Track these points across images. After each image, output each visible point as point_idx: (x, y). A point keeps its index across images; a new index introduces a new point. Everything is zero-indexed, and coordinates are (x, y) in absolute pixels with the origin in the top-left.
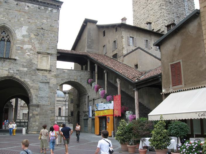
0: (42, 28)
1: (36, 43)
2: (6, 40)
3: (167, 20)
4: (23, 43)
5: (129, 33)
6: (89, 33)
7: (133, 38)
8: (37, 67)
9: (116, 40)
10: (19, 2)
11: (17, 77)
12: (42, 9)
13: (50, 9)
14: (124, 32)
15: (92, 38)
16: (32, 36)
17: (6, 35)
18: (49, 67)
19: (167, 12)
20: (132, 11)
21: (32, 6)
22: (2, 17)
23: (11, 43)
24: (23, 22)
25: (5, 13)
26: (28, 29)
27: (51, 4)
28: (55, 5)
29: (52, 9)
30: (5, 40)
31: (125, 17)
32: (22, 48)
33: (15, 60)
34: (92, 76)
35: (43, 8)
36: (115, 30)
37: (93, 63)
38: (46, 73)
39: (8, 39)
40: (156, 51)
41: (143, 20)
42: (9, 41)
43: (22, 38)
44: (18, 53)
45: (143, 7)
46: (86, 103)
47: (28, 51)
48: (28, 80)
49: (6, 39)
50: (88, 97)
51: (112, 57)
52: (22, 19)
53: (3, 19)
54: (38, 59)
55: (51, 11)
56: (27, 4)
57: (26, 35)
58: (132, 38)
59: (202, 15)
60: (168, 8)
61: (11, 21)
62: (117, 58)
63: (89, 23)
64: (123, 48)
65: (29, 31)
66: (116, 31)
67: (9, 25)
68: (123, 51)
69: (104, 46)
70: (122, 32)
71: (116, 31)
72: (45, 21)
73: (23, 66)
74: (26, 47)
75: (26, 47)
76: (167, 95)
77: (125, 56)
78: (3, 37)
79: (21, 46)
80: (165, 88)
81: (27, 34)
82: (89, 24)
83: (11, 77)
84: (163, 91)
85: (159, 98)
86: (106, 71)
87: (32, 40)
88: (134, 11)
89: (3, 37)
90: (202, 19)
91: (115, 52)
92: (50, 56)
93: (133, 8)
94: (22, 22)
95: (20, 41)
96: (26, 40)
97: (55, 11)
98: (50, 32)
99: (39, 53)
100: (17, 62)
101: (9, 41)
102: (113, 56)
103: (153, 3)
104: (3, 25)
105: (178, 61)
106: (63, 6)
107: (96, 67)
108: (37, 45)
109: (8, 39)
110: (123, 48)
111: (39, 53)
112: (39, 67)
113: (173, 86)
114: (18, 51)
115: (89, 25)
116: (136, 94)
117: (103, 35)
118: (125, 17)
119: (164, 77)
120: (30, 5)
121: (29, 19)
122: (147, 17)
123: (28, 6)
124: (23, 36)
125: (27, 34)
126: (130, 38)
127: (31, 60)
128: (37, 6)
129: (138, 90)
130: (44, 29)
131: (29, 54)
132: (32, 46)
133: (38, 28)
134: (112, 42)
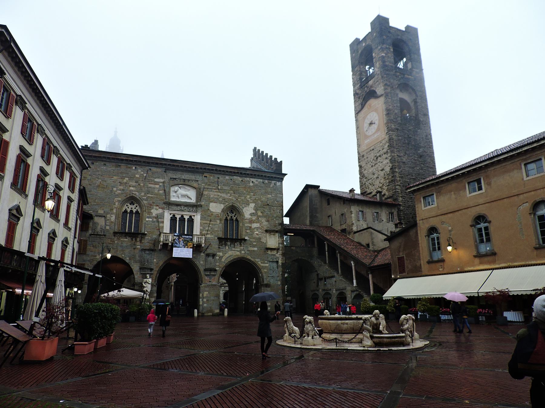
0: (268, 204)
1: (263, 220)
2: (234, 220)
3: (399, 186)
4: (251, 222)
5: (358, 207)
6: (311, 201)
7: (362, 212)
8: (266, 246)
9: (344, 213)
10: (243, 178)
11: (249, 257)
12: (266, 183)
13: (273, 182)
14: (353, 206)
15: (314, 206)
16: (259, 213)
17: (234, 215)
19: (400, 175)
20: (358, 166)
21: (257, 181)
23: (239, 223)
24: (249, 199)
25: (232, 192)
26: (255, 206)
27: (275, 178)
28: (278, 178)
29: (275, 182)
30: (233, 219)
31: (353, 189)
32: (250, 227)
33: (245, 240)
34: (321, 253)
35: (266, 181)
36: (342, 203)
37: (322, 240)
38: (274, 252)
40: (388, 224)
41: (372, 180)
42: (237, 220)
43: (250, 217)
44: (248, 233)
45: (372, 164)
46: (314, 281)
48: (259, 260)
49: (234, 218)
50: (318, 275)
51: (340, 231)
52: (249, 196)
53: (230, 198)
54: (266, 238)
55: (275, 184)
56: (252, 180)
57: (253, 213)
58: (361, 212)
59: (418, 225)
60: (400, 170)
61: (238, 200)
62: (346, 233)
63: (311, 189)
64: (353, 224)
65: (256, 209)
66: (344, 204)
67: (237, 205)
68: (353, 227)
69: (329, 216)
70: (350, 207)
71: (344, 204)
72: (270, 196)
73: (254, 246)
75: (255, 225)
76: (395, 280)
77: (355, 233)
78: (231, 217)
79: (250, 225)
80: (393, 275)
81: (254, 211)
82: (310, 190)
83: (243, 258)
84: (393, 276)
85: (390, 283)
86: (339, 251)
87: (260, 218)
88: (360, 167)
89: (231, 217)
90: (419, 228)
91: (344, 227)
92: (277, 234)
93: (359, 162)
94: (248, 199)
95: (248, 219)
97: (278, 184)
98: (275, 208)
99: (267, 231)
100: (247, 242)
102: (341, 230)
103: (384, 163)
104: (231, 204)
105: (402, 256)
106: (285, 178)
107: (326, 245)
108: (265, 223)
109: (236, 218)
110: (353, 224)
111: (267, 231)
112: (268, 246)
113: (400, 273)
114: (248, 231)
115: (311, 192)
116: (370, 276)
117: (327, 204)
118: (353, 189)
119: (393, 267)
120: (254, 180)
121: (255, 195)
122: (377, 178)
123: (252, 182)
124: (251, 214)
125: (254, 211)
126: (359, 212)
127: (260, 239)
128: (261, 180)
129: (371, 273)
130: (270, 206)
131: (258, 233)
132: (260, 225)
133: (264, 204)
134: (338, 215)
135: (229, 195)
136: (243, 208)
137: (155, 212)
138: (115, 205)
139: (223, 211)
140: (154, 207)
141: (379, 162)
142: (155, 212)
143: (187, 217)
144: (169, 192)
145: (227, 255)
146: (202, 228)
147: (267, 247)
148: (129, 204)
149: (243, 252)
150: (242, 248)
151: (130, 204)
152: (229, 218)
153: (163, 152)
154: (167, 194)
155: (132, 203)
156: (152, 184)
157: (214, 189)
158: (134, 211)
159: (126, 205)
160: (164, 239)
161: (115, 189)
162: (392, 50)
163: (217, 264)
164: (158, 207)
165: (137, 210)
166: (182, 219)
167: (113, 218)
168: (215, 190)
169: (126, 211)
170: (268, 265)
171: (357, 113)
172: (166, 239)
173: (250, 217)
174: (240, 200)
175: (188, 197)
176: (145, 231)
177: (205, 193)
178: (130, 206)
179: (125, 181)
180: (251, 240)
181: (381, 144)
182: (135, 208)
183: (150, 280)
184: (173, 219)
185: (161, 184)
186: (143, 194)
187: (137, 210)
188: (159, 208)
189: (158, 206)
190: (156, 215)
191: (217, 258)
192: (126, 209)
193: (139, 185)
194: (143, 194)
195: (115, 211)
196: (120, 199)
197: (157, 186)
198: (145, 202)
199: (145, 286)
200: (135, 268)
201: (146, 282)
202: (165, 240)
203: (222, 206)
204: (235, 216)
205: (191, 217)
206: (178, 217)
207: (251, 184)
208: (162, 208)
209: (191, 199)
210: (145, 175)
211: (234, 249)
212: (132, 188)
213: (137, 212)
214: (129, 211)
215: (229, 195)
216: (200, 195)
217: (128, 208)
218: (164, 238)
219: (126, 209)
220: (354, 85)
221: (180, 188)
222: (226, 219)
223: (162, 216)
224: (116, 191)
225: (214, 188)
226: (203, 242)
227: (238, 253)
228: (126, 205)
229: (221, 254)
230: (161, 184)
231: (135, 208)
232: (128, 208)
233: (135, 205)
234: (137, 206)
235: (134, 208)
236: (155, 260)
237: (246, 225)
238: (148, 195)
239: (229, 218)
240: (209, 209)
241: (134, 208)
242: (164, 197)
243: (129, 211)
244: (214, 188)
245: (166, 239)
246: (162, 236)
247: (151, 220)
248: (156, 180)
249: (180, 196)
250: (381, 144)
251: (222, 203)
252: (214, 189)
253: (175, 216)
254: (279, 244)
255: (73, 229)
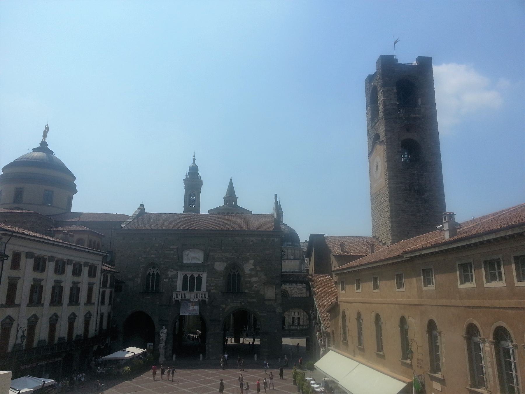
4: (251, 276)
16: (258, 268)
18: (274, 296)
22: (231, 255)
32: (250, 281)
33: (245, 293)
39: (238, 273)
42: (239, 275)
43: (249, 272)
47: (256, 283)
52: (248, 254)
53: (232, 256)
57: (253, 269)
61: (239, 258)
65: (255, 265)
72: (268, 252)
74: (254, 279)
75: (254, 279)
78: (234, 272)
81: (253, 267)
89: (234, 272)
96: (253, 273)
101: (239, 275)
109: (238, 273)
124: (251, 270)
125: (253, 267)
128: (260, 238)
131: (256, 286)
135: (231, 254)
136: (244, 264)
137: (170, 274)
138: (140, 270)
139: (226, 268)
140: (170, 270)
141: (382, 209)
142: (170, 274)
143: (196, 276)
144: (182, 257)
145: (229, 307)
146: (208, 284)
147: (265, 298)
148: (151, 269)
149: (243, 304)
150: (242, 300)
151: (153, 268)
152: (232, 274)
153: (231, 177)
154: (180, 257)
155: (154, 268)
156: (168, 251)
157: (219, 250)
158: (156, 273)
159: (149, 269)
160: (176, 297)
161: (140, 258)
162: (395, 91)
163: (221, 315)
164: (173, 269)
165: (158, 272)
166: (192, 277)
167: (139, 281)
168: (219, 251)
169: (149, 274)
170: (266, 314)
171: (370, 154)
172: (177, 297)
173: (249, 272)
174: (241, 257)
175: (197, 259)
176: (162, 290)
177: (211, 254)
178: (152, 270)
179: (148, 250)
180: (251, 292)
181: (383, 191)
182: (156, 271)
183: (166, 331)
184: (185, 278)
185: (175, 250)
186: (161, 259)
187: (158, 272)
188: (174, 270)
189: (172, 268)
190: (172, 276)
191: (221, 309)
192: (149, 273)
193: (158, 252)
194: (161, 259)
195: (140, 275)
196: (144, 265)
197: (172, 252)
198: (163, 266)
199: (162, 335)
200: (156, 320)
201: (162, 333)
202: (176, 298)
203: (225, 264)
204: (237, 272)
205: (199, 275)
206: (189, 276)
207: (251, 243)
208: (177, 270)
209: (200, 260)
210: (163, 243)
211: (235, 301)
212: (153, 256)
213: (158, 274)
214: (151, 273)
215: (231, 254)
216: (207, 257)
217: (151, 271)
218: (176, 296)
219: (149, 273)
220: (368, 124)
221: (190, 251)
222: (230, 275)
223: (176, 276)
224: (141, 260)
225: (218, 249)
226: (207, 297)
227: (239, 305)
228: (149, 269)
229: (224, 306)
230: (175, 250)
231: (156, 271)
232: (151, 271)
233: (156, 268)
234: (157, 270)
235: (155, 271)
236: (171, 313)
237: (246, 279)
238: (165, 260)
239: (232, 274)
240: (213, 268)
241: (155, 271)
242: (178, 260)
243: (151, 274)
244: (218, 249)
245: (177, 297)
246: (174, 294)
247: (167, 280)
248: (172, 247)
249: (190, 258)
250: (383, 191)
251: (224, 262)
252: (219, 250)
253: (186, 275)
254: (276, 295)
255: (96, 303)
